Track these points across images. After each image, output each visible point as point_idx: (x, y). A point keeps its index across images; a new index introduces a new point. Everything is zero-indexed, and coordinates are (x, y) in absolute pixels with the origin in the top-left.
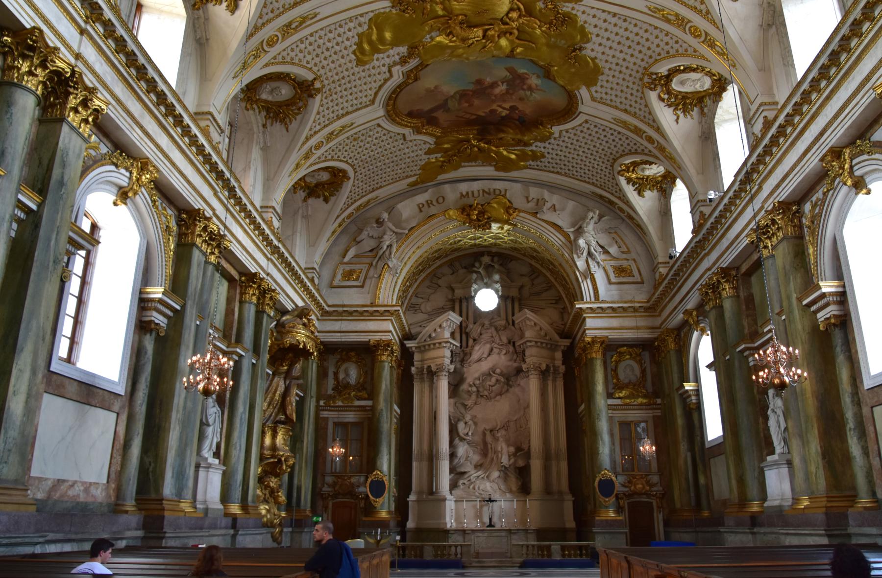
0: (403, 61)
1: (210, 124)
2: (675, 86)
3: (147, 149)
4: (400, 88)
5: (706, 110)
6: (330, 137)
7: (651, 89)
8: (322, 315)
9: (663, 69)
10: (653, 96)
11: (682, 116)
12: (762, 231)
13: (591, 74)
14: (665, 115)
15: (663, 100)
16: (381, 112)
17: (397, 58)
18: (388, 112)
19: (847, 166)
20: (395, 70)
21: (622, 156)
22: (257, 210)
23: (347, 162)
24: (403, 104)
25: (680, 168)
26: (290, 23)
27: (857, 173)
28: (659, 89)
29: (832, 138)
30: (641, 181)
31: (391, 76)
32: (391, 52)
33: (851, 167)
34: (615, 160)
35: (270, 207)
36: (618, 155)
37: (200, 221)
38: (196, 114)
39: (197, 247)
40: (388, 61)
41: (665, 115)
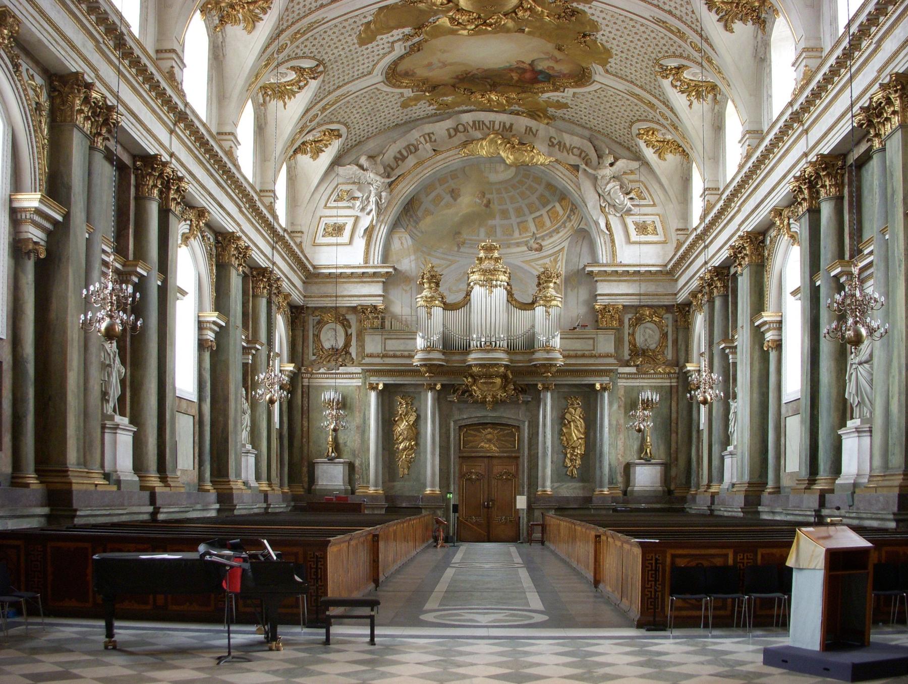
0: (407, 38)
1: (174, 65)
2: (686, 75)
3: (202, 200)
4: (402, 58)
5: (718, 97)
6: (324, 109)
7: (663, 77)
8: (306, 278)
9: (672, 63)
10: (666, 83)
11: (695, 102)
12: (737, 251)
13: (604, 55)
14: (679, 100)
15: (676, 87)
16: (380, 78)
17: (401, 36)
18: (387, 78)
19: (786, 222)
20: (396, 45)
21: (638, 120)
22: (256, 192)
23: (339, 122)
24: (401, 68)
25: (729, 86)
26: (299, 31)
27: (792, 230)
28: (671, 78)
29: (776, 199)
30: (661, 144)
31: (393, 49)
32: (395, 32)
33: (789, 224)
34: (632, 123)
35: (229, 134)
36: (635, 119)
37: (173, 184)
38: (219, 134)
39: (234, 267)
40: (391, 39)
41: (679, 100)
